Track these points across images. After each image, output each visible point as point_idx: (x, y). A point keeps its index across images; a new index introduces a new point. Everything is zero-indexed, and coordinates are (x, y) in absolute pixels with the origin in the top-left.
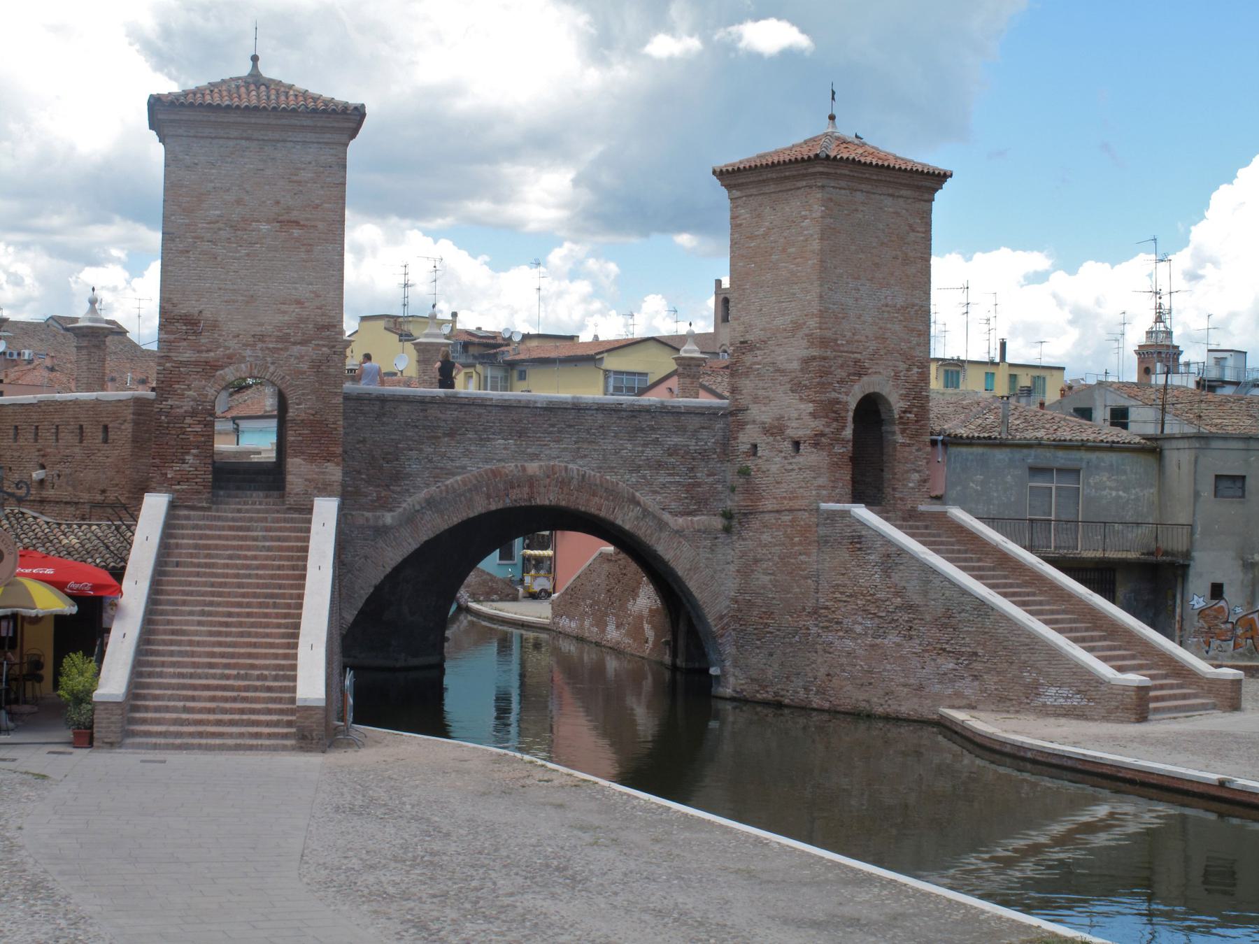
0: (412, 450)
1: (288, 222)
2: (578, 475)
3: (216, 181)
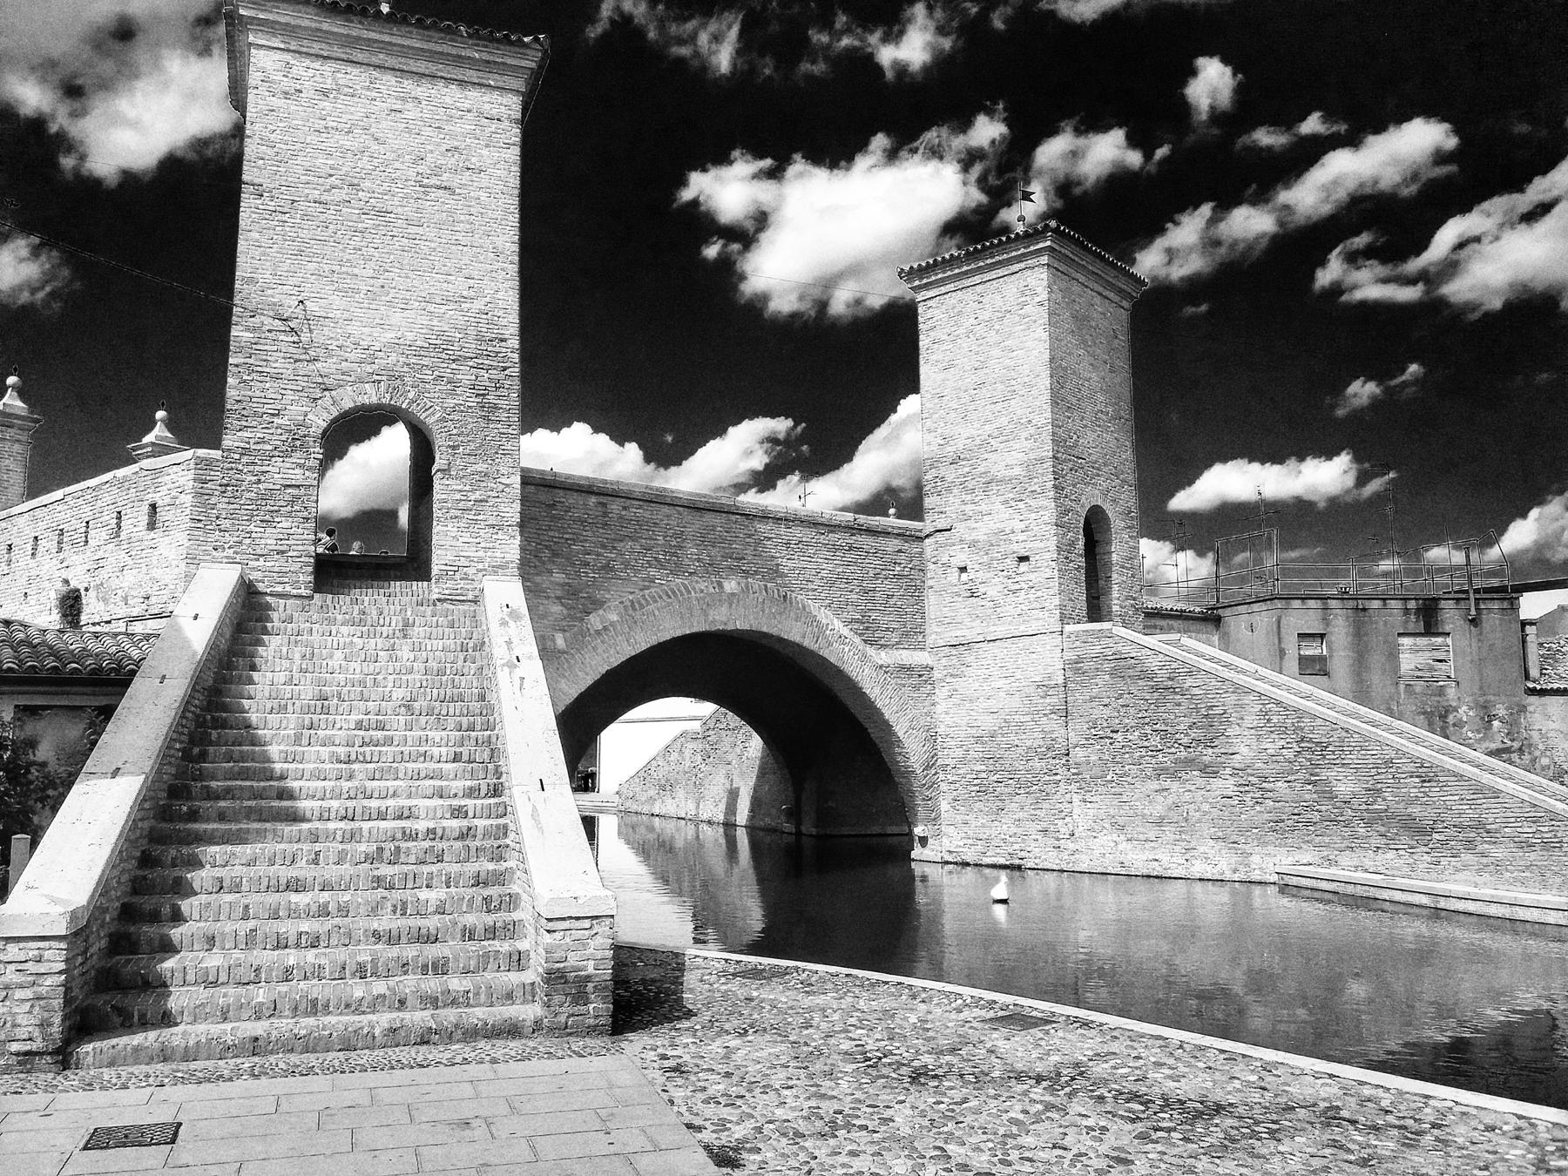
0: (589, 554)
1: (439, 188)
2: (779, 596)
3: (328, 118)
